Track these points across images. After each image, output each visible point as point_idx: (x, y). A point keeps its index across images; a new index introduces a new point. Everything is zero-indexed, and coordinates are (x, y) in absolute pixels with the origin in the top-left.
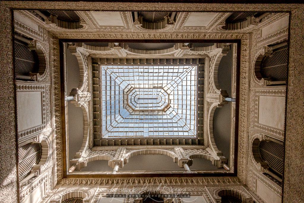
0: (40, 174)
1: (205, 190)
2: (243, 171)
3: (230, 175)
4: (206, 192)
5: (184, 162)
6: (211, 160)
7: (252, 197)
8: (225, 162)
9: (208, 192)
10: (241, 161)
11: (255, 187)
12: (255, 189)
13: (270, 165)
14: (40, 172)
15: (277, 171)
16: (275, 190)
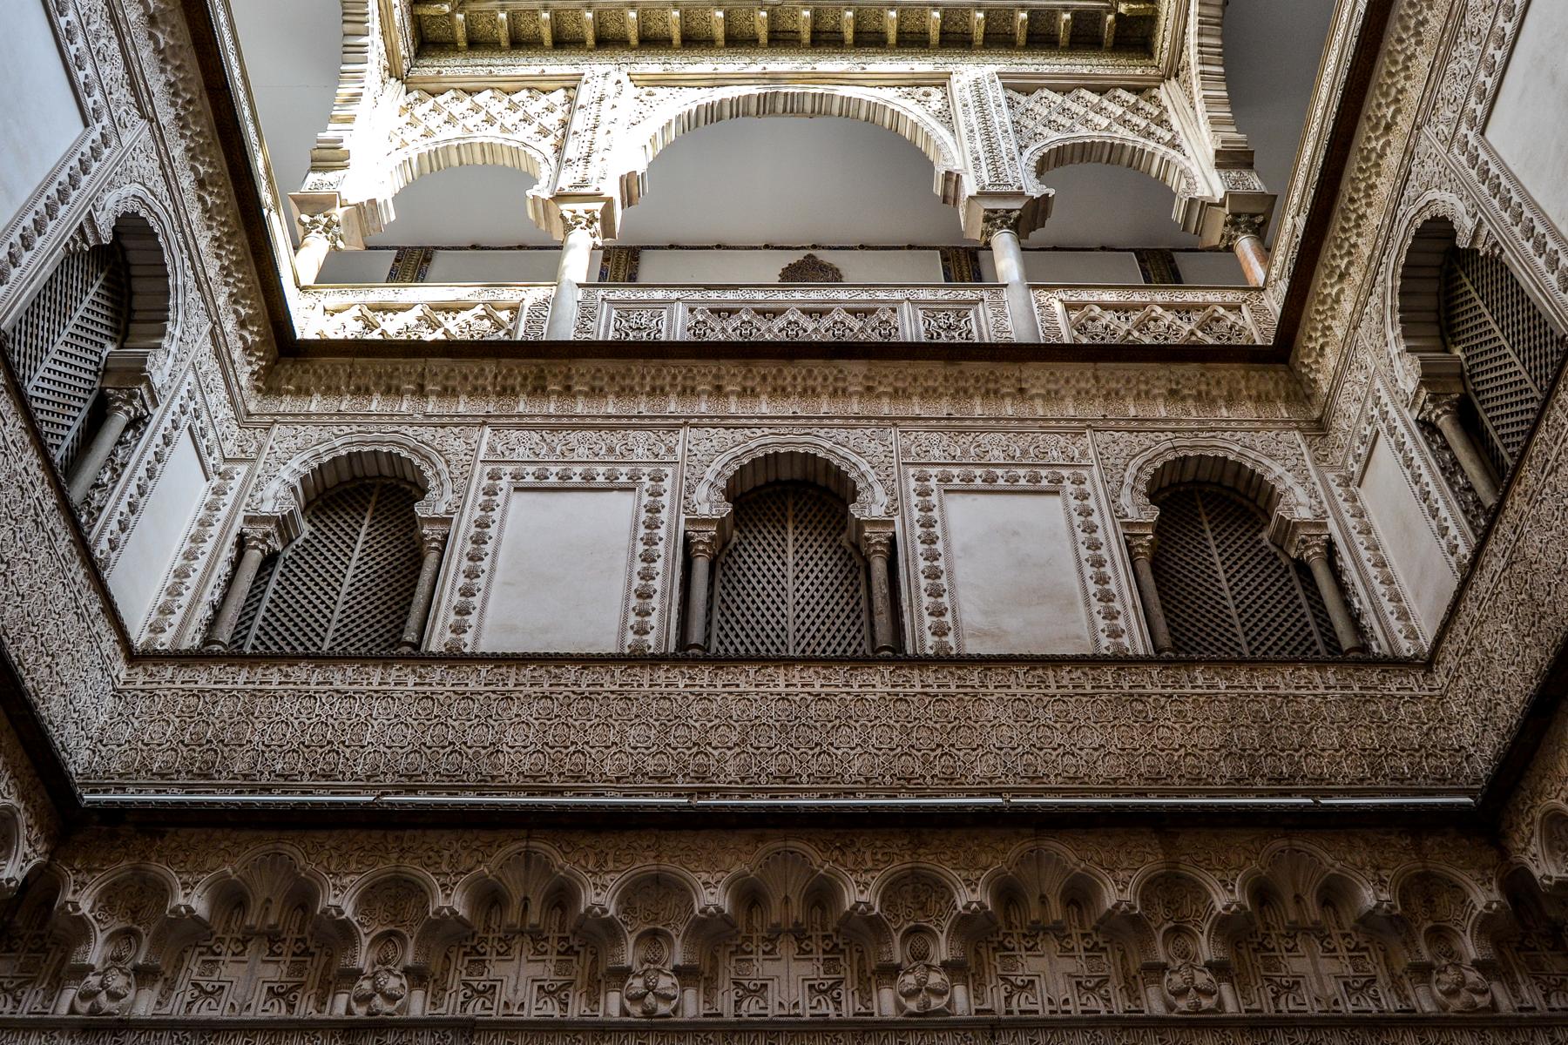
0: (156, 405)
1: (1083, 454)
2: (1328, 350)
3: (1250, 355)
4: (1085, 473)
5: (995, 211)
6: (1173, 180)
7: (1329, 512)
8: (1253, 215)
9: (1095, 469)
10: (1374, 149)
11: (1363, 459)
12: (1356, 468)
13: (1472, 377)
14: (150, 389)
15: (1496, 428)
16: (1444, 531)
